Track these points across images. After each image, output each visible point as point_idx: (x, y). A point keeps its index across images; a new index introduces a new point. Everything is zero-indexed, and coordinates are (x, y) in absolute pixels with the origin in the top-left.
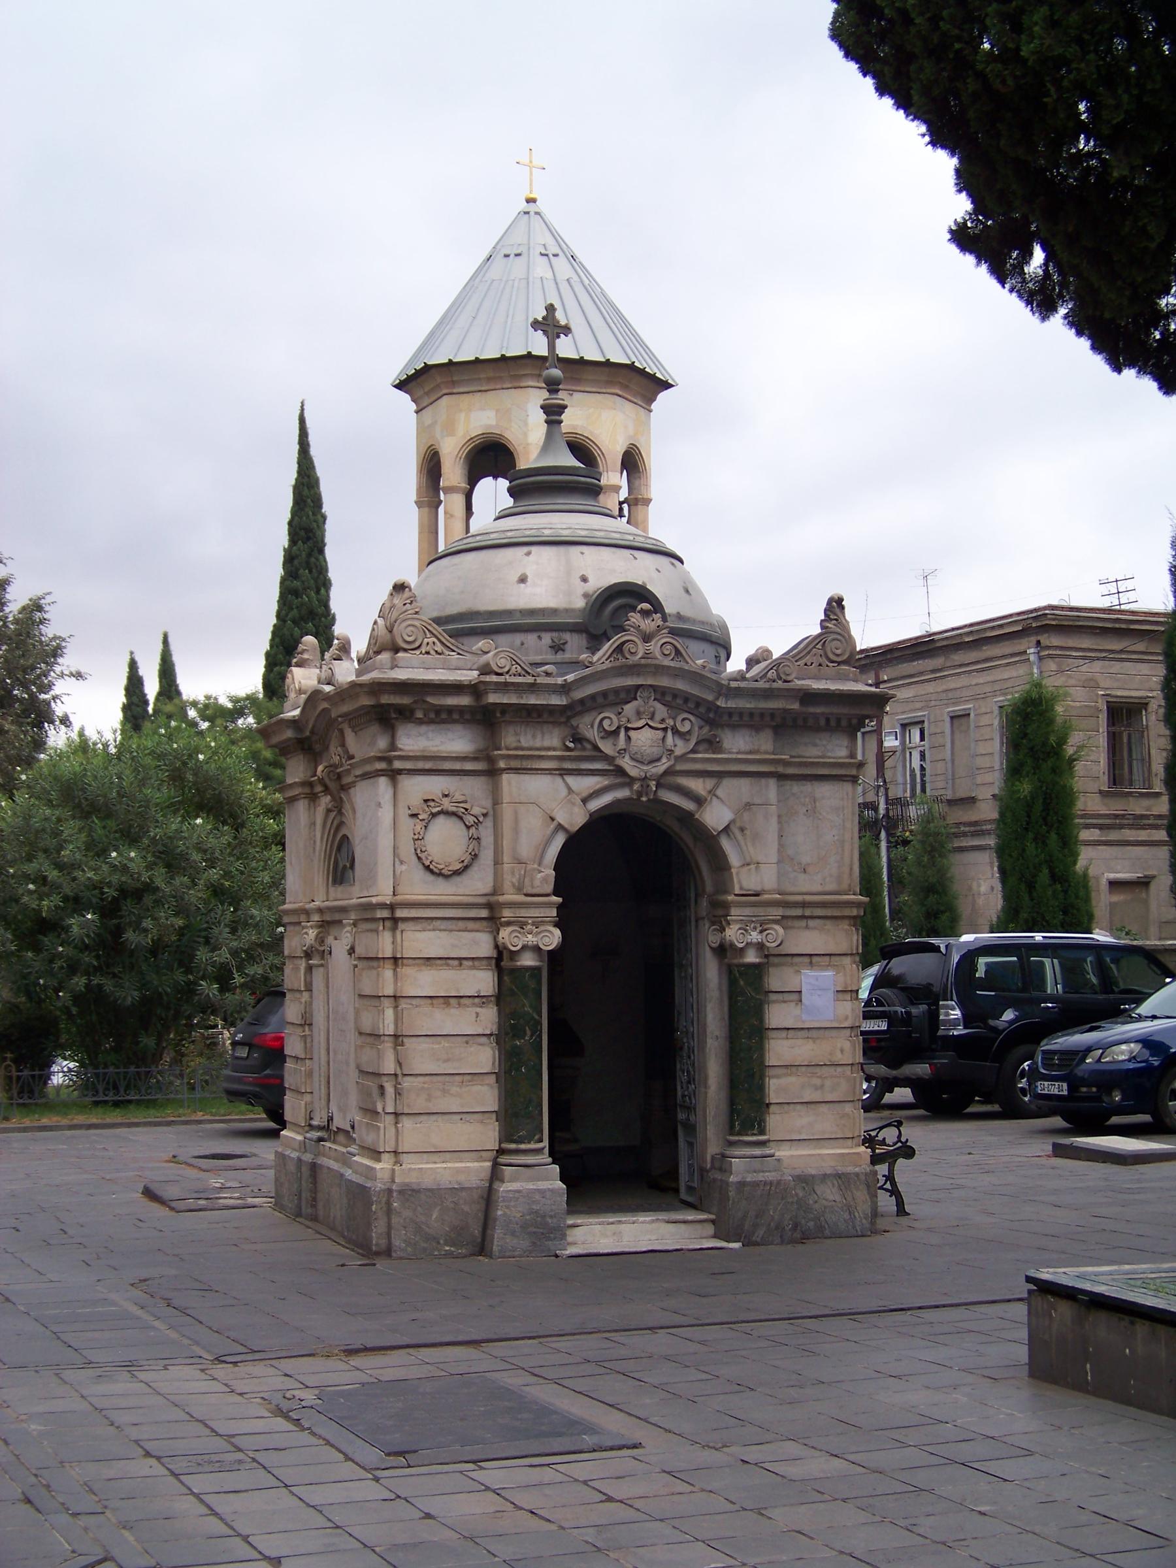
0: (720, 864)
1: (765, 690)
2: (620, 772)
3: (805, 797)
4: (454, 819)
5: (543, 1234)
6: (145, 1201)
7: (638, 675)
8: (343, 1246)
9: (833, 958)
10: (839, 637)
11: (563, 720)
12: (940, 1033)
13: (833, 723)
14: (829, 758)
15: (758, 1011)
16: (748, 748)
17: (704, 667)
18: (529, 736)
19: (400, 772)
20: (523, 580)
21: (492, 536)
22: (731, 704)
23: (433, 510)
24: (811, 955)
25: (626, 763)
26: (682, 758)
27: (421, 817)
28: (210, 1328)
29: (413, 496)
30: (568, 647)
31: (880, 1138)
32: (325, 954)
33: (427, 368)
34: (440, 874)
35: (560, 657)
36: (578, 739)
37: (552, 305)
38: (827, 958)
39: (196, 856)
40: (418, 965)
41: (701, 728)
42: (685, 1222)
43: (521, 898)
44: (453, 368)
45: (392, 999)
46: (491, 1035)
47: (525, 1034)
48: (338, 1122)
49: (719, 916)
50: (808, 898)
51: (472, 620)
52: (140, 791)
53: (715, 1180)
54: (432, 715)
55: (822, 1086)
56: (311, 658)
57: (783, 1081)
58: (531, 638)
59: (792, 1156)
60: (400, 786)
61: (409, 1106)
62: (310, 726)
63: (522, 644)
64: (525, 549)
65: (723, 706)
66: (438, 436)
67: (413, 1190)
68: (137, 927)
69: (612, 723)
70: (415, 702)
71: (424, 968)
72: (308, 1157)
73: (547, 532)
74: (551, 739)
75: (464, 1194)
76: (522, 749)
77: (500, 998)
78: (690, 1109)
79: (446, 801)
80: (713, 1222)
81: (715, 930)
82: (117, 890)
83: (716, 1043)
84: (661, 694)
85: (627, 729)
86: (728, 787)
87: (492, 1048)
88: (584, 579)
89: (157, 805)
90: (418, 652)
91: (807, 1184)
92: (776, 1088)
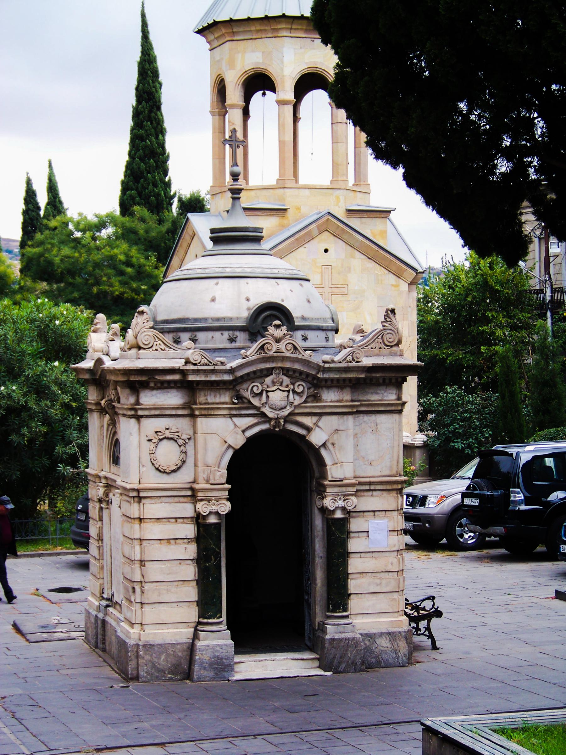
0: (322, 463)
1: (345, 368)
2: (263, 415)
3: (371, 423)
4: (172, 441)
5: (221, 668)
6: (13, 631)
7: (273, 362)
8: (116, 672)
9: (387, 512)
10: (391, 332)
11: (231, 387)
12: (510, 508)
13: (387, 381)
14: (385, 400)
15: (344, 544)
16: (336, 399)
17: (311, 356)
18: (212, 396)
19: (142, 416)
20: (213, 300)
22: (326, 376)
23: (222, 117)
24: (374, 511)
25: (267, 410)
26: (299, 406)
27: (153, 441)
28: (32, 734)
29: (209, 108)
30: (238, 339)
31: (422, 606)
32: (109, 503)
33: (215, 23)
34: (164, 472)
35: (233, 345)
36: (240, 398)
37: (235, 129)
38: (384, 512)
39: (55, 388)
40: (154, 522)
41: (309, 389)
42: (302, 660)
43: (208, 486)
44: (233, 24)
45: (139, 541)
46: (193, 559)
47: (211, 560)
48: (115, 599)
49: (321, 491)
50: (372, 480)
51: (185, 322)
52: (19, 346)
53: (319, 636)
54: (159, 385)
55: (381, 583)
56: (101, 327)
58: (217, 334)
59: (363, 623)
60: (142, 424)
61: (148, 599)
62: (99, 374)
63: (213, 338)
64: (215, 281)
65: (321, 377)
66: (224, 68)
67: (151, 645)
68: (17, 432)
69: (258, 388)
70: (149, 379)
71: (156, 524)
72: (101, 616)
73: (228, 270)
74: (225, 397)
75: (179, 646)
76: (209, 404)
77: (198, 539)
78: (309, 594)
79: (167, 432)
80: (318, 659)
81: (319, 498)
82: (4, 410)
83: (321, 561)
84: (286, 372)
85: (267, 392)
86: (326, 421)
87: (194, 566)
88: (248, 300)
89: (29, 354)
90: (151, 350)
91: (371, 638)
92: (354, 585)
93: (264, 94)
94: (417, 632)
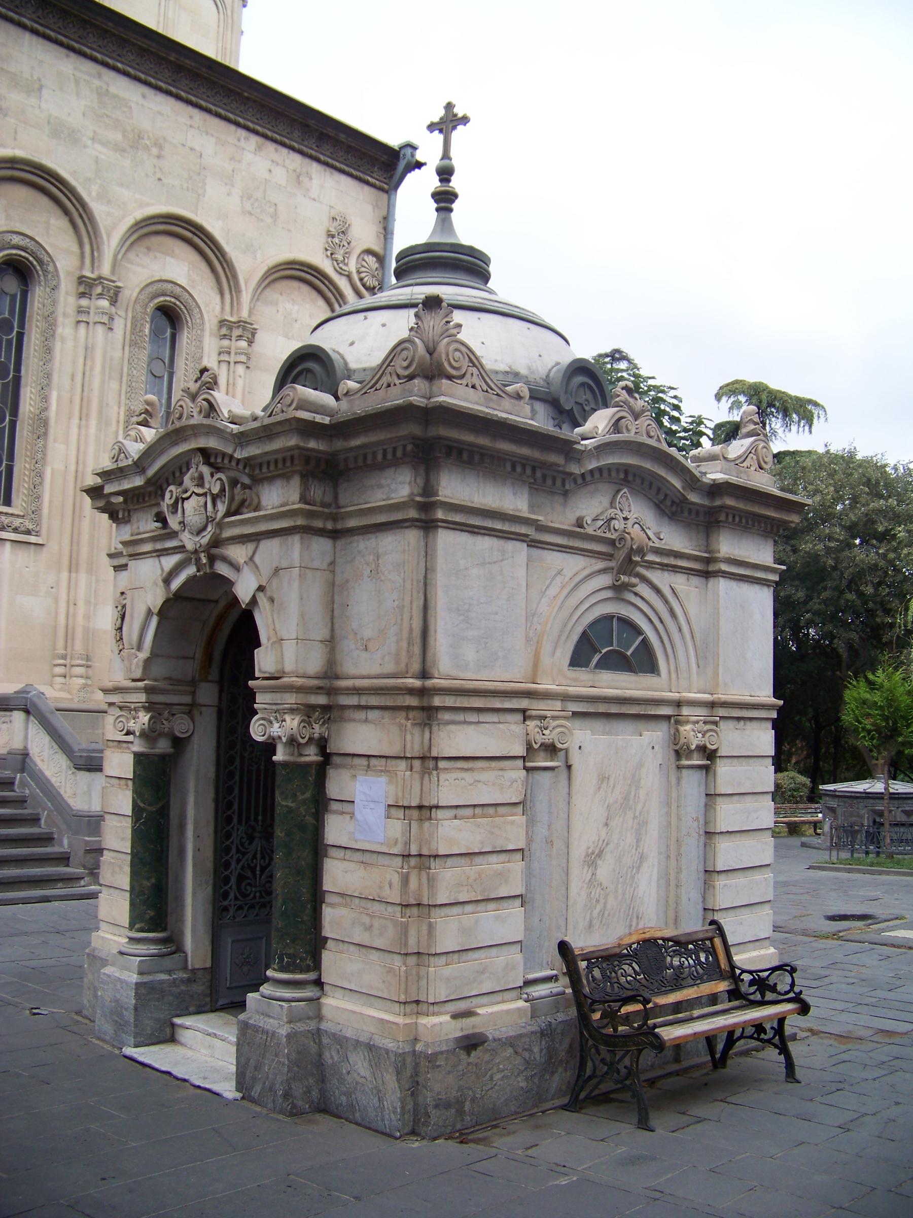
3: (370, 554)
24: (369, 756)
55: (371, 926)
57: (343, 912)
94: (759, 1035)
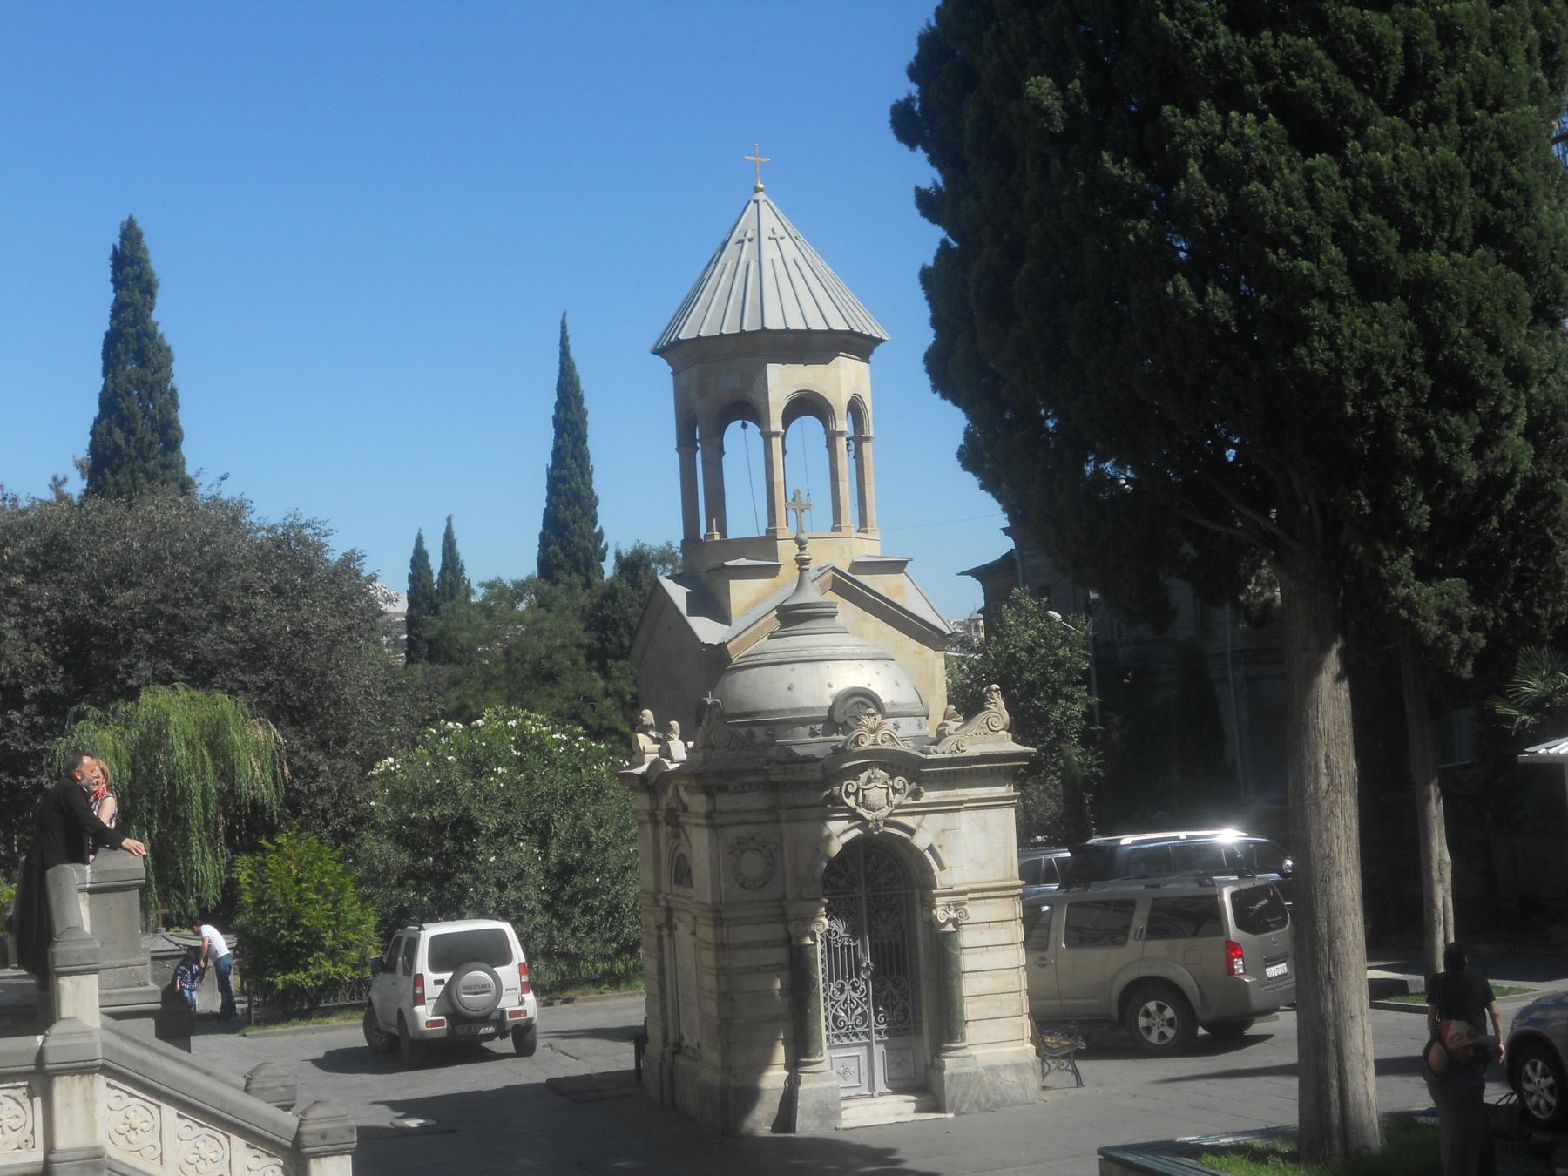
21: (769, 656)
64: (791, 666)
73: (804, 653)
93: (744, 426)
